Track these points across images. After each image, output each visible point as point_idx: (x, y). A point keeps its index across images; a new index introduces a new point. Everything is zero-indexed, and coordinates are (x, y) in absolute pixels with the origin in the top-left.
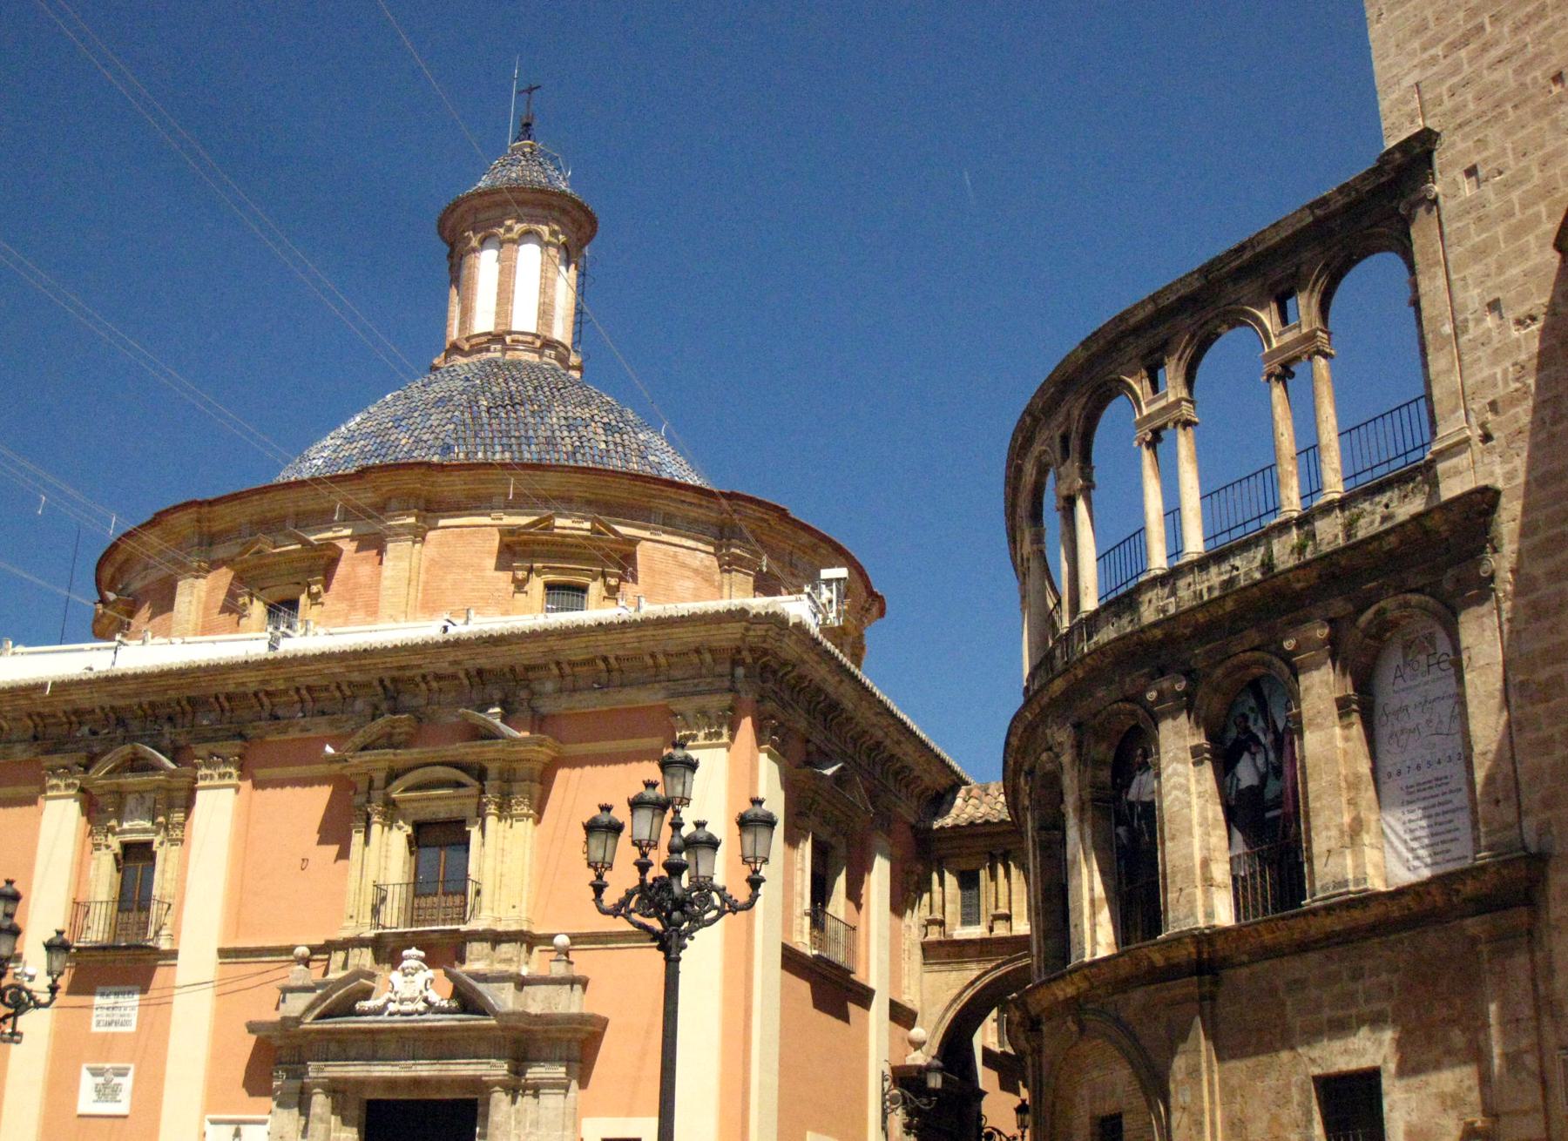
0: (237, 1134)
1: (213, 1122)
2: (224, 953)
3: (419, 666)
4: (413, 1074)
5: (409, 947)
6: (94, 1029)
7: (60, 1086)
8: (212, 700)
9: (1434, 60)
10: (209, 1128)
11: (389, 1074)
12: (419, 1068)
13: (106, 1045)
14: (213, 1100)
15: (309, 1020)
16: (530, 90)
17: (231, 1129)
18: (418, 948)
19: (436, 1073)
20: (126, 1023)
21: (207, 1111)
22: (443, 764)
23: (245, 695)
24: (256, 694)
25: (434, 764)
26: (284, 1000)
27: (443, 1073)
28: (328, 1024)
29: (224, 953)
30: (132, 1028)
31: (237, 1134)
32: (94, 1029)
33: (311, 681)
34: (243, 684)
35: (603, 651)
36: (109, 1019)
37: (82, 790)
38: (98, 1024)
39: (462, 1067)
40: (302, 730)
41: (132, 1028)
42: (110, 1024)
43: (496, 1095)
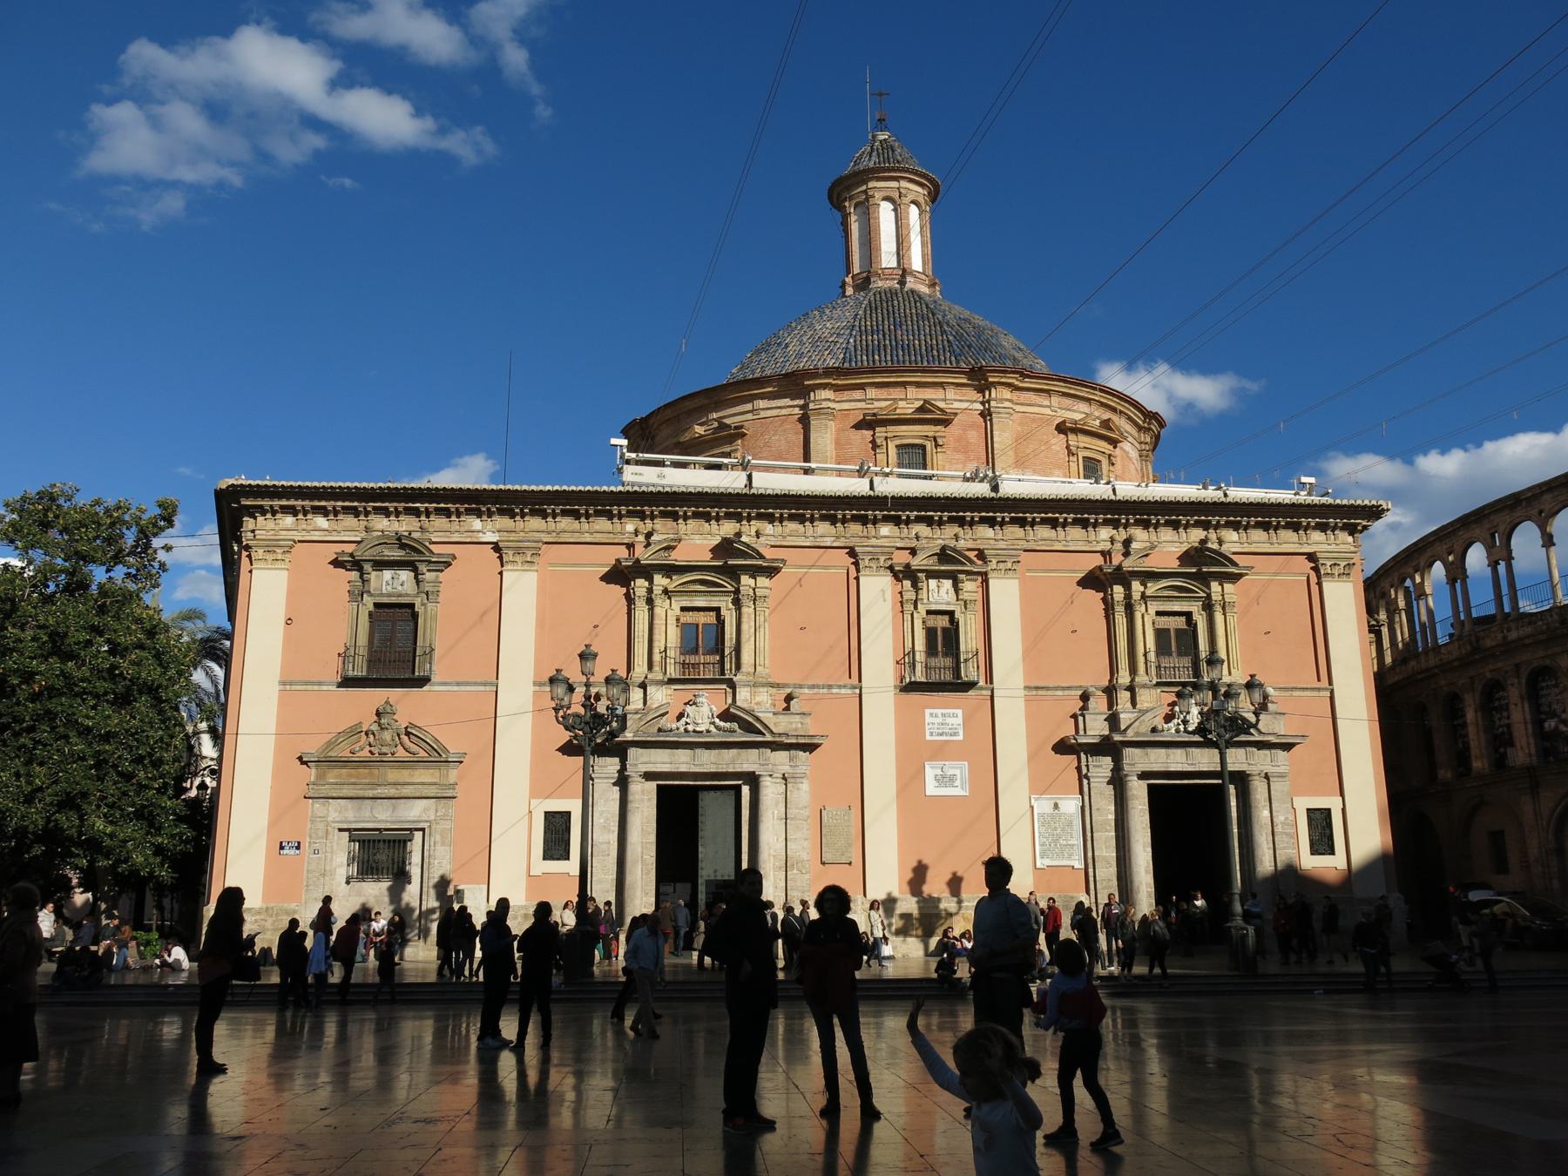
0: (1056, 806)
4: (1197, 769)
6: (928, 737)
7: (909, 778)
13: (940, 751)
14: (1040, 786)
16: (881, 94)
20: (955, 734)
30: (960, 737)
31: (1056, 806)
32: (928, 737)
36: (941, 731)
37: (891, 568)
38: (931, 734)
40: (1065, 546)
41: (960, 737)
42: (941, 735)
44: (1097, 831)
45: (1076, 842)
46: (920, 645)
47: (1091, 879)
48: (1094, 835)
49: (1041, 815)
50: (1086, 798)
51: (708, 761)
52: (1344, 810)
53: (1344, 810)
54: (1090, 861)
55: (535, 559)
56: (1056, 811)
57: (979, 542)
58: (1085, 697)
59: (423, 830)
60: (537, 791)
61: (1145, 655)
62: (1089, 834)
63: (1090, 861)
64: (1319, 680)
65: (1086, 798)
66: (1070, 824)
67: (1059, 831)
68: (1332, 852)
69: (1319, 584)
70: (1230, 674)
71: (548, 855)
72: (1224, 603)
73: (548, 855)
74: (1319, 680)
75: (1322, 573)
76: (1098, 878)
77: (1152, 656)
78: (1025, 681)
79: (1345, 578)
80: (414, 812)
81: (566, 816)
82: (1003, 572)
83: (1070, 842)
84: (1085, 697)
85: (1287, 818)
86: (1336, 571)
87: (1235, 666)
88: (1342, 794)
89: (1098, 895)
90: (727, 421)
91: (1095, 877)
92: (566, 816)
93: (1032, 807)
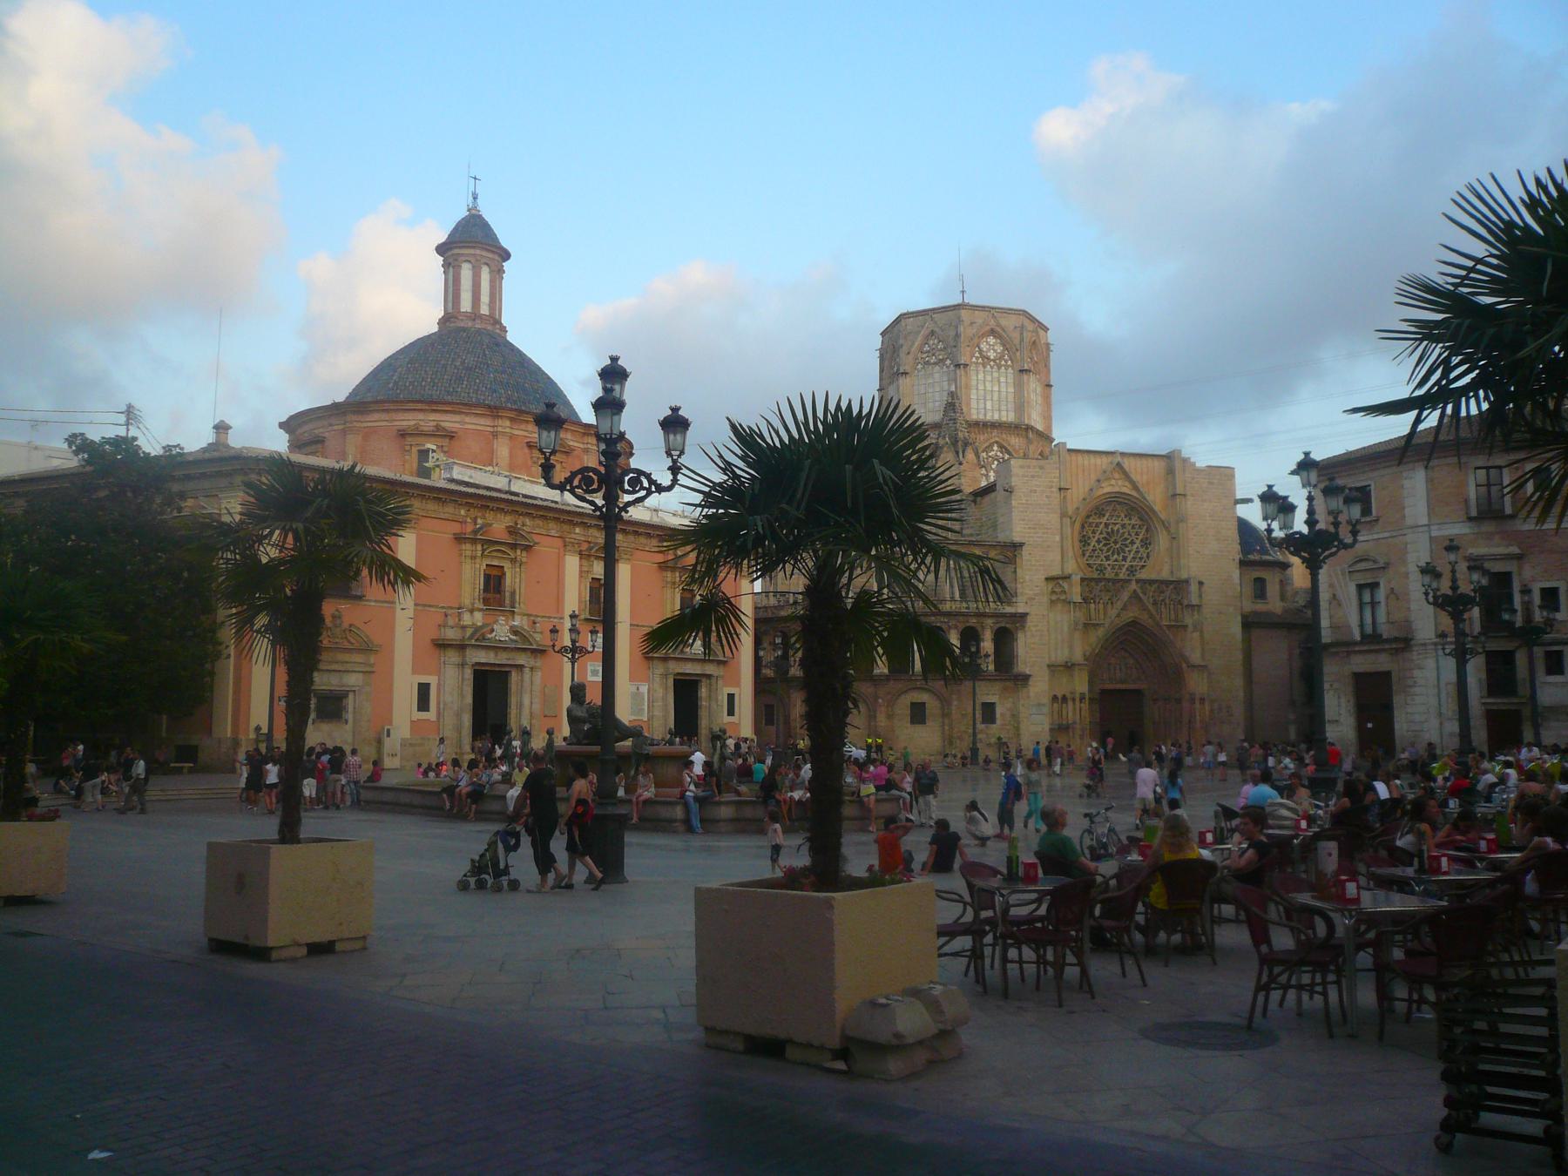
9: (1025, 528)
14: (632, 679)
31: (638, 689)
46: (588, 598)
51: (502, 658)
52: (740, 695)
53: (740, 695)
55: (416, 526)
59: (354, 691)
60: (415, 671)
66: (643, 696)
71: (420, 709)
73: (420, 709)
80: (353, 680)
81: (428, 685)
90: (443, 424)
92: (428, 685)
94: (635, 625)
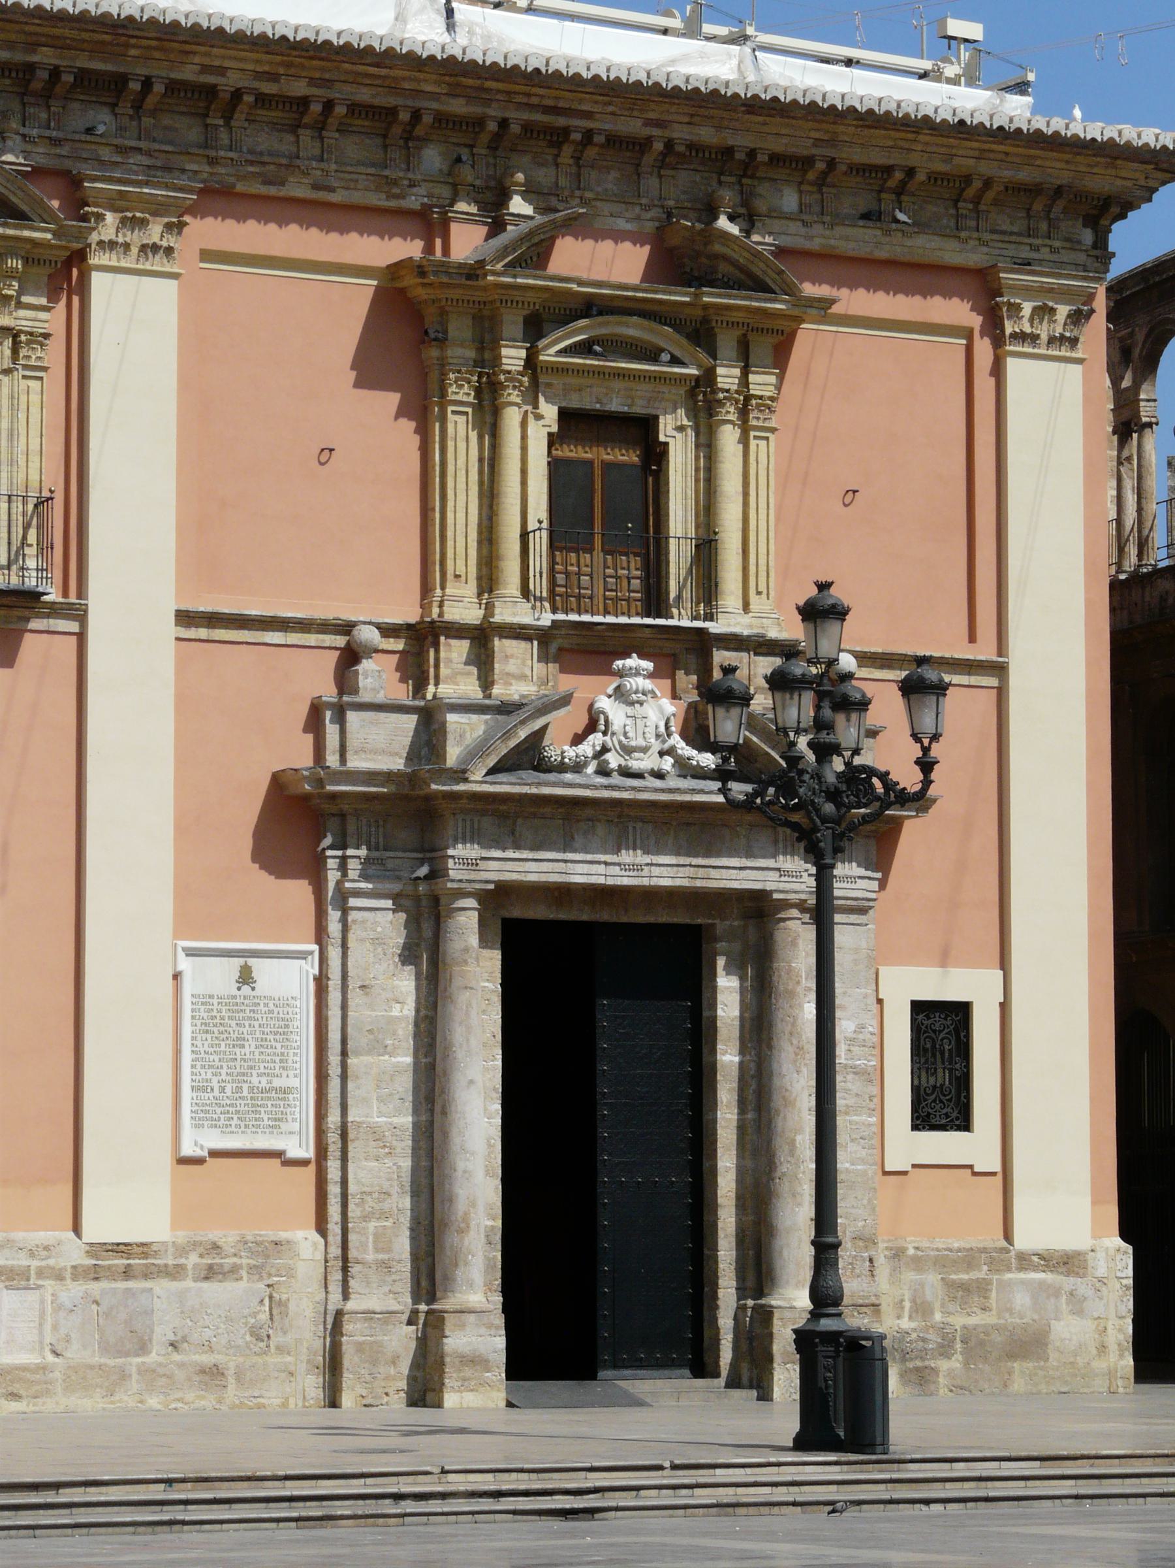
0: (246, 977)
1: (191, 953)
2: (185, 618)
3: (589, 115)
4: (645, 882)
5: (626, 655)
8: (135, 86)
10: (185, 964)
11: (601, 880)
12: (656, 871)
15: (478, 774)
17: (238, 962)
18: (642, 656)
19: (685, 883)
21: (178, 934)
22: (643, 314)
23: (211, 92)
24: (237, 95)
25: (630, 312)
26: (314, 722)
27: (698, 883)
28: (505, 785)
29: (185, 618)
31: (246, 977)
33: (364, 95)
34: (222, 71)
35: (914, 160)
39: (733, 873)
40: (316, 187)
43: (790, 924)
44: (357, 1054)
45: (295, 1083)
47: (334, 1190)
48: (352, 1061)
49: (203, 1000)
50: (334, 954)
52: (1005, 1008)
53: (1005, 1008)
54: (333, 1138)
56: (246, 989)
57: (65, 150)
58: (351, 657)
61: (524, 535)
62: (334, 1059)
63: (333, 1138)
64: (972, 639)
65: (334, 954)
66: (284, 1031)
67: (250, 1047)
68: (963, 1123)
69: (998, 371)
70: (746, 607)
72: (748, 398)
74: (972, 639)
75: (1009, 330)
76: (352, 1188)
77: (540, 542)
78: (182, 586)
79: (1064, 352)
82: (135, 250)
83: (277, 1083)
84: (351, 657)
85: (861, 1027)
86: (1044, 332)
87: (762, 587)
88: (1004, 963)
89: (352, 1237)
91: (344, 1182)
93: (177, 976)
94: (213, 620)
